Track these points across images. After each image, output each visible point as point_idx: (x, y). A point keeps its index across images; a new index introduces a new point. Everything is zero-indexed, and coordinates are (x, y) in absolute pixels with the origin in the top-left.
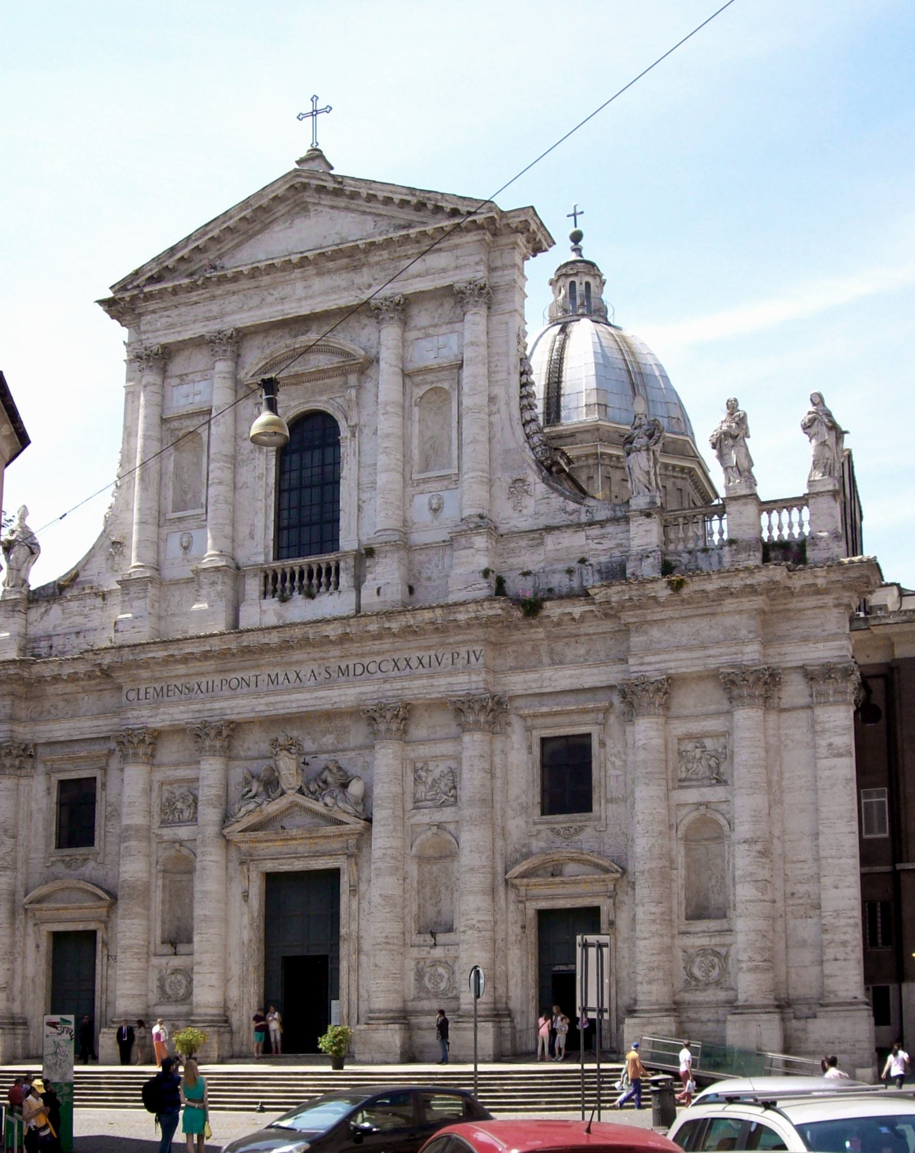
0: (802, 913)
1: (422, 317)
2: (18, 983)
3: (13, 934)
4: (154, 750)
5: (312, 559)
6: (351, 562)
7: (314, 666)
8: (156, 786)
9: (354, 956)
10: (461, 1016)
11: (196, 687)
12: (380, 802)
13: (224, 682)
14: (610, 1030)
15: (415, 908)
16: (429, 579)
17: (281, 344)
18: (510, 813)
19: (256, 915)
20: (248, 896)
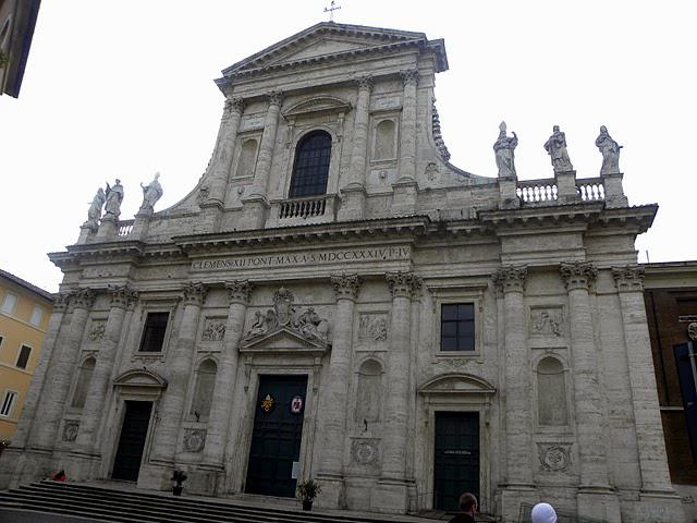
0: (620, 424)
1: (380, 89)
2: (100, 432)
3: (104, 400)
4: (204, 298)
5: (311, 198)
6: (333, 200)
7: (306, 254)
8: (202, 319)
10: (381, 479)
14: (486, 498)
15: (354, 405)
16: (377, 212)
18: (420, 348)
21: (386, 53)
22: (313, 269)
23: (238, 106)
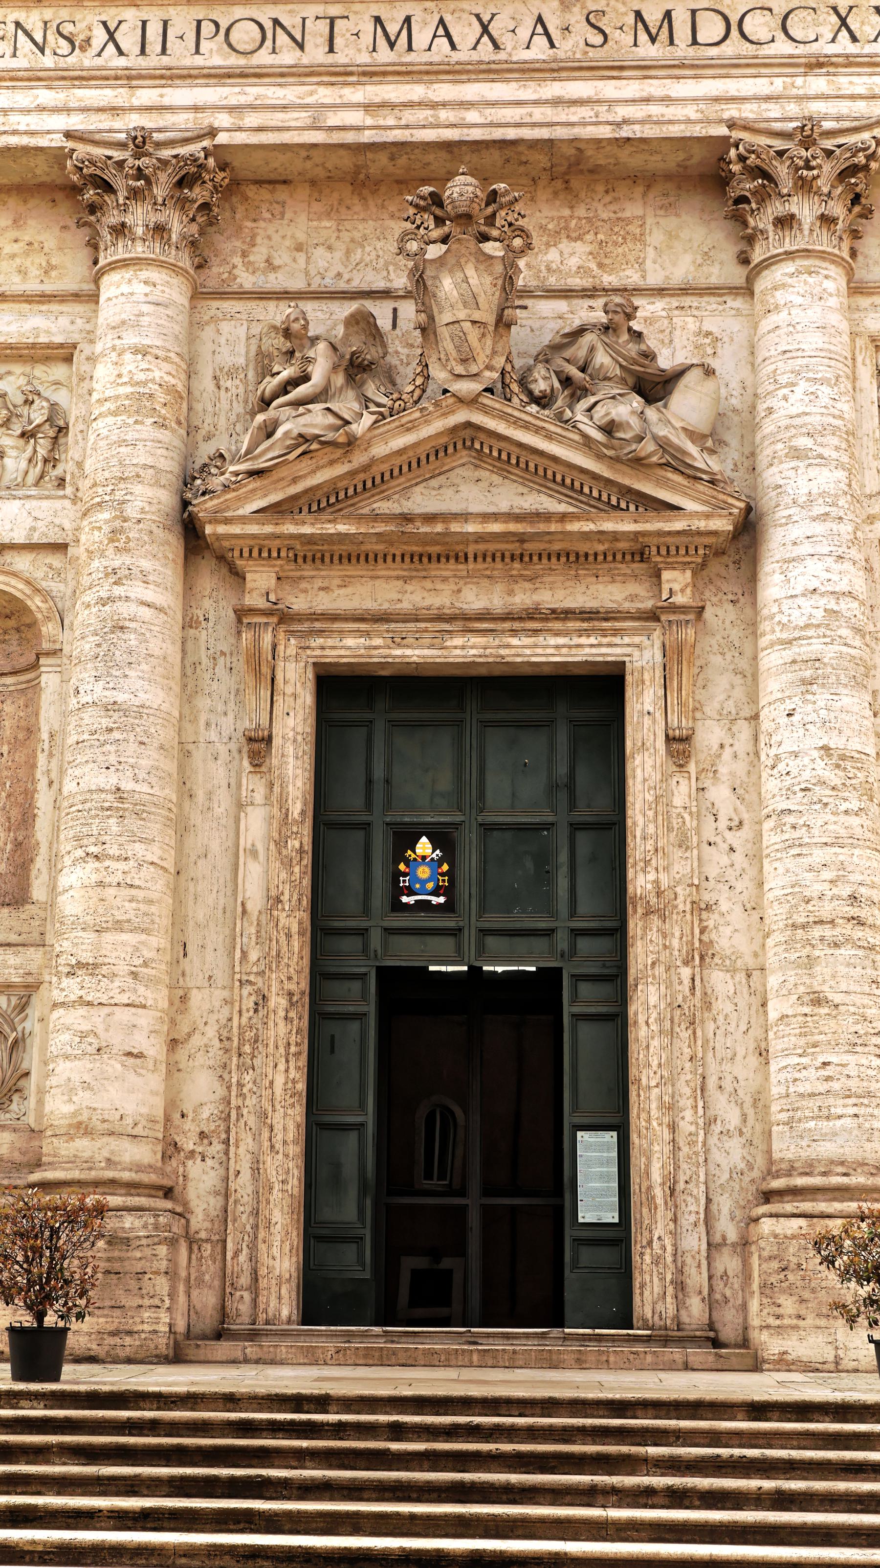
9: (686, 973)
11: (100, 36)
12: (804, 442)
13: (207, 29)
19: (296, 809)
20: (269, 740)
22: (609, 89)
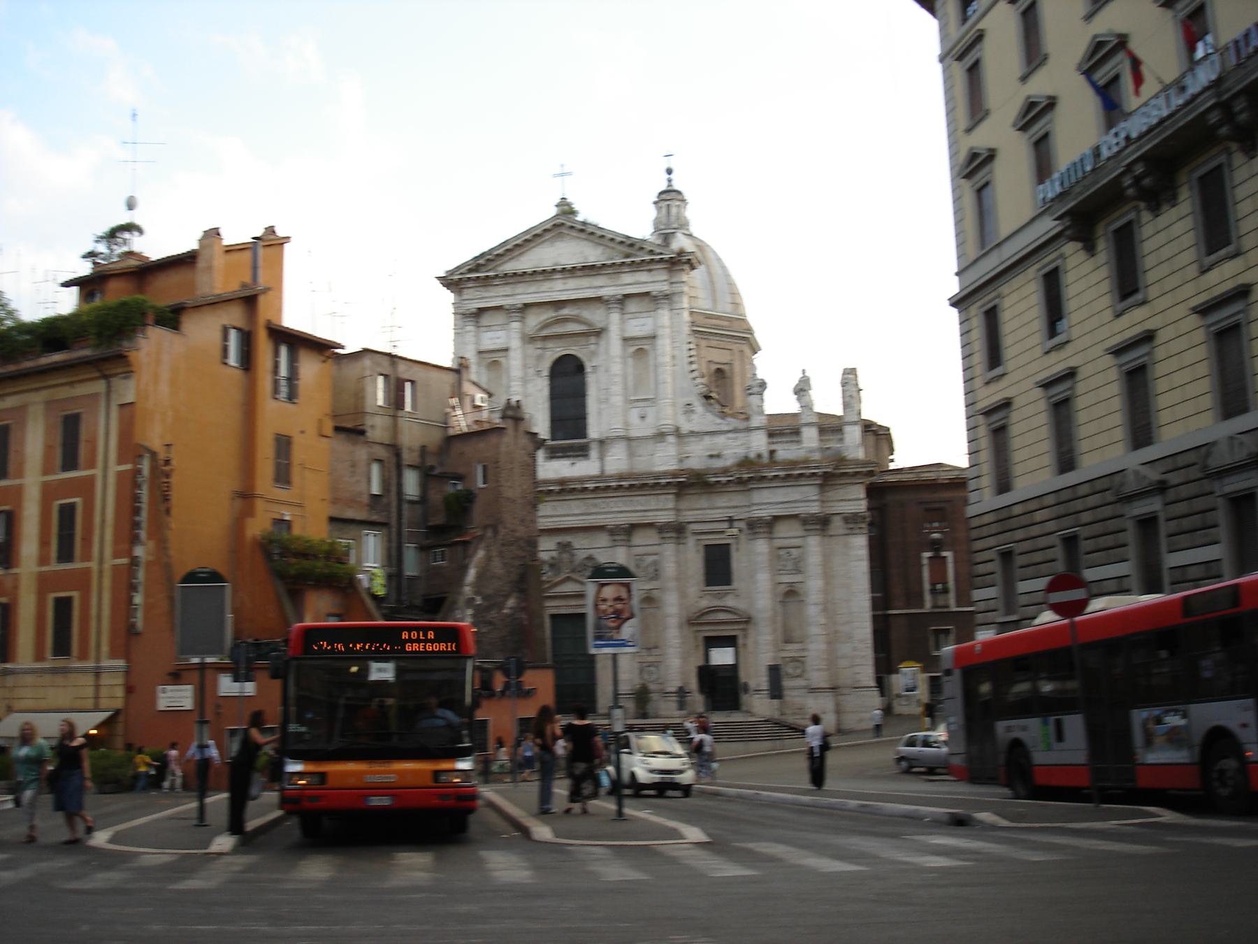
17: (549, 314)
21: (636, 267)
23: (472, 317)
